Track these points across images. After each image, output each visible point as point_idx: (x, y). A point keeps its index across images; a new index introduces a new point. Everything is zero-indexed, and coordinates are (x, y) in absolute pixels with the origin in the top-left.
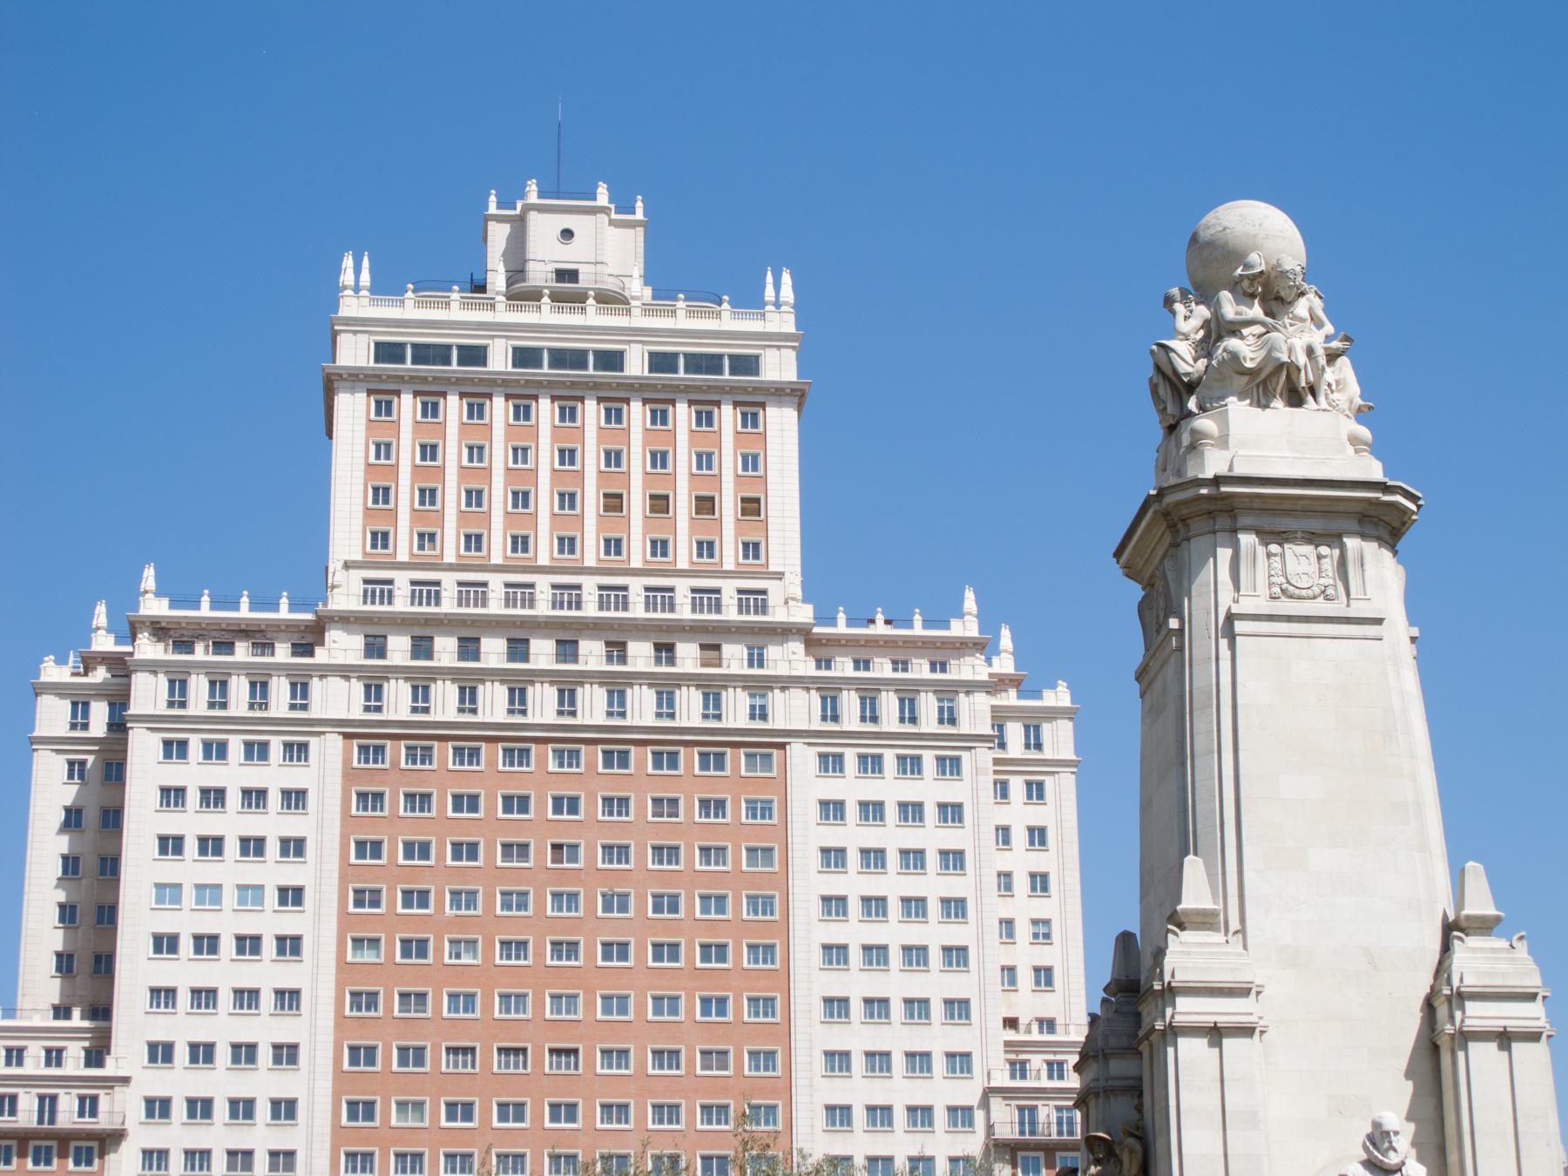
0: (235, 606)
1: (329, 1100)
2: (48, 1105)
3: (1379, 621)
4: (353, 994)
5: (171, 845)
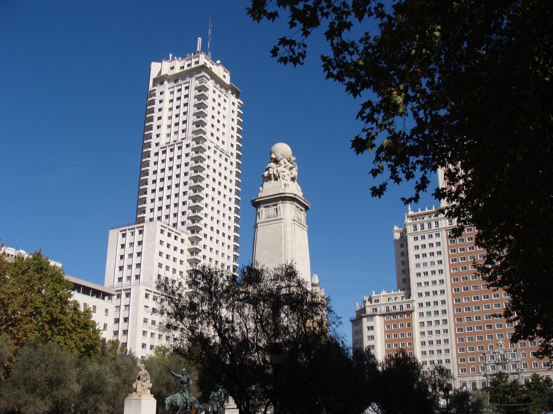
0: (425, 210)
2: (401, 307)
3: (281, 219)
5: (417, 256)
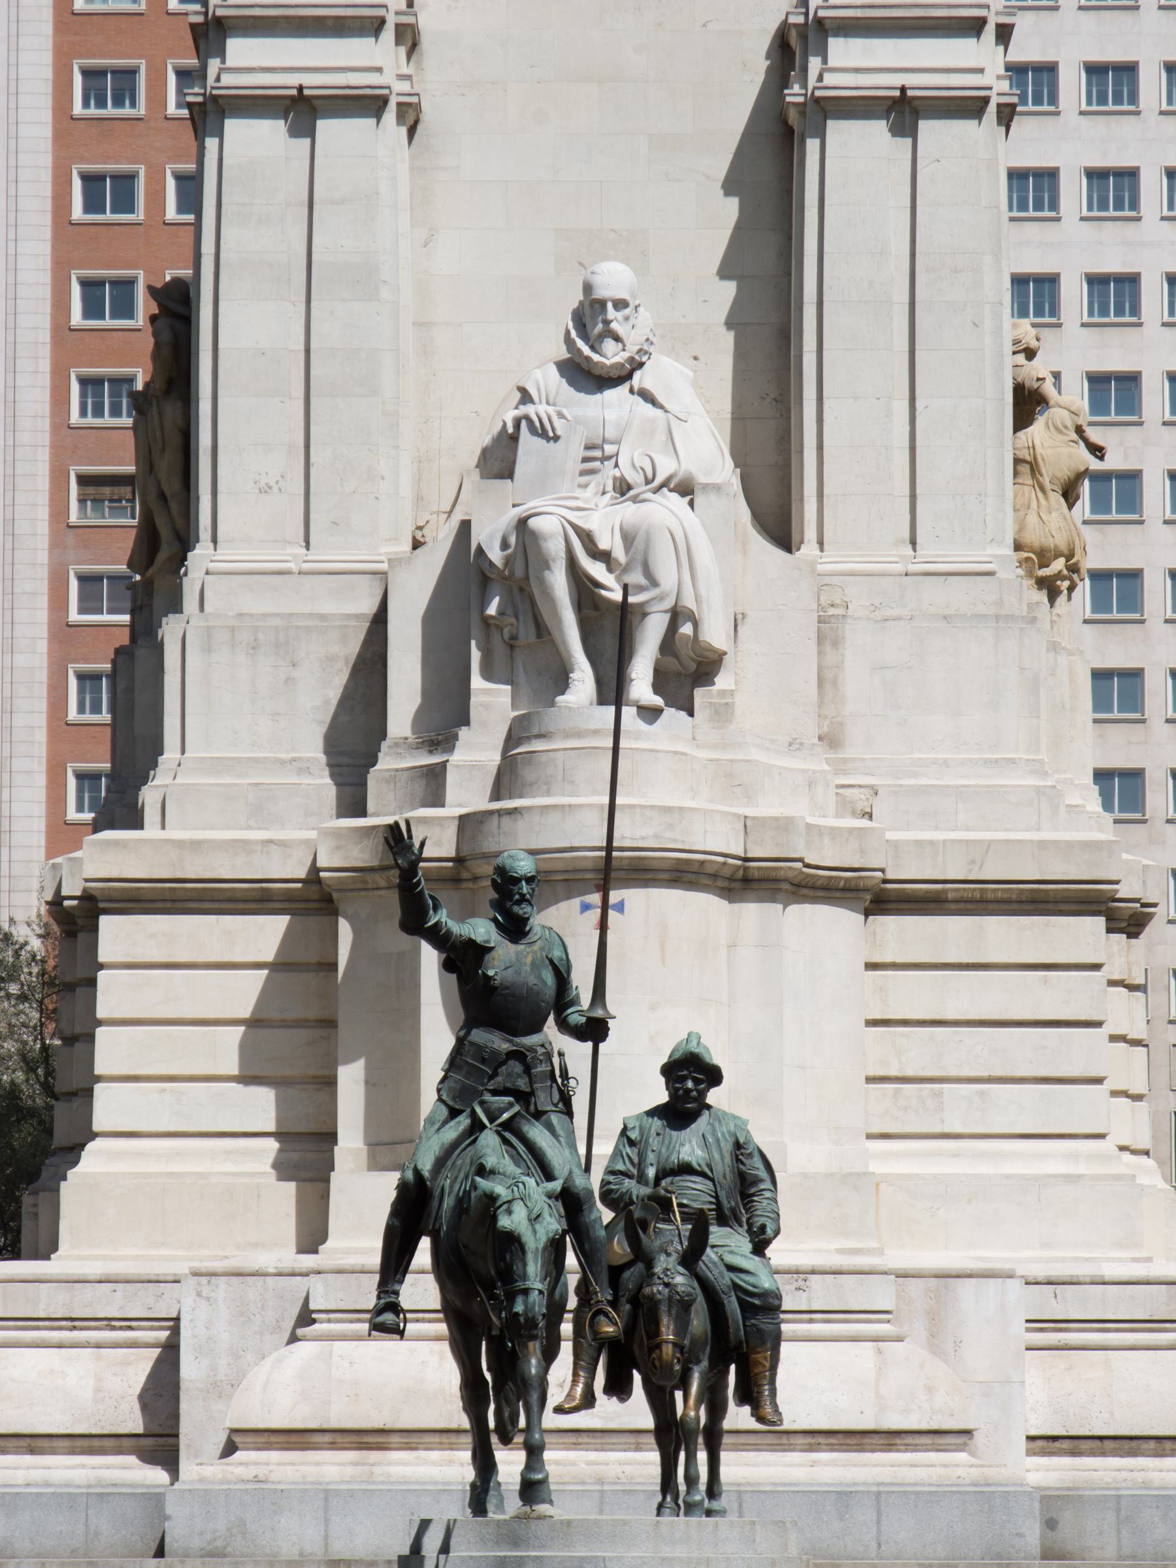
1: (46, 278)
4: (87, 73)
